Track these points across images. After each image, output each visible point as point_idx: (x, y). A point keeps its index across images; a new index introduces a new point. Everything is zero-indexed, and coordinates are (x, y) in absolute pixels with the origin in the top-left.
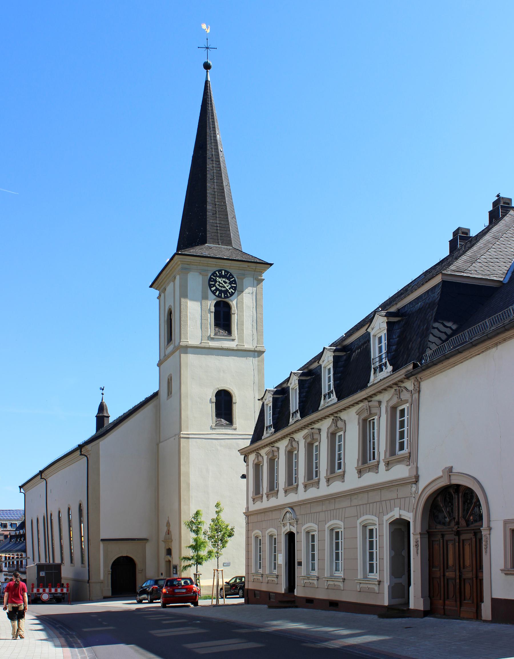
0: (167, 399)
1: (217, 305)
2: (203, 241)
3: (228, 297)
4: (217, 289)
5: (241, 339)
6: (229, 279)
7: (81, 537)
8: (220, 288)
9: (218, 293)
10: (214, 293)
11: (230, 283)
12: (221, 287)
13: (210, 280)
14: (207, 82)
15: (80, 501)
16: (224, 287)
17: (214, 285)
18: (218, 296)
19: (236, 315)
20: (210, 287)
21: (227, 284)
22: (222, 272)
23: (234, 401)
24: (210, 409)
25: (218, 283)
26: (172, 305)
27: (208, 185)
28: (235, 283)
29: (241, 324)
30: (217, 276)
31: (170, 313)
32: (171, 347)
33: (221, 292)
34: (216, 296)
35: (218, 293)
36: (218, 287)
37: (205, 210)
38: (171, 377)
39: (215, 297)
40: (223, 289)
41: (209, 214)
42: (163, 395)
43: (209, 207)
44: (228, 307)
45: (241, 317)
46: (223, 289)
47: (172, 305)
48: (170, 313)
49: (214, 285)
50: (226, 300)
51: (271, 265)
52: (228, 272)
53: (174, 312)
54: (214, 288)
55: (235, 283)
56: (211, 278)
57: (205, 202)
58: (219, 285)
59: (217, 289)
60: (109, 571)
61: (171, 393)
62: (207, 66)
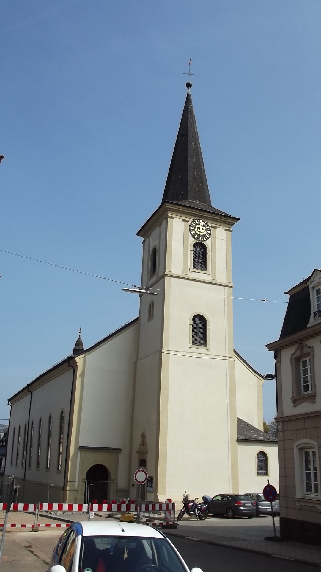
0: (148, 321)
1: (196, 245)
2: (185, 198)
4: (196, 233)
5: (214, 274)
7: (60, 443)
8: (198, 233)
9: (196, 236)
10: (193, 236)
11: (206, 230)
15: (63, 409)
17: (194, 230)
19: (210, 255)
20: (190, 232)
23: (208, 325)
24: (188, 330)
25: (196, 229)
26: (157, 245)
27: (189, 159)
28: (210, 231)
29: (214, 262)
31: (155, 251)
32: (155, 279)
35: (196, 236)
37: (187, 176)
38: (153, 303)
39: (194, 239)
41: (190, 179)
42: (144, 320)
43: (190, 175)
44: (204, 247)
45: (214, 257)
47: (157, 245)
48: (155, 251)
49: (194, 230)
51: (238, 219)
53: (159, 251)
54: (193, 232)
55: (210, 231)
56: (191, 224)
57: (187, 170)
60: (83, 479)
61: (153, 316)
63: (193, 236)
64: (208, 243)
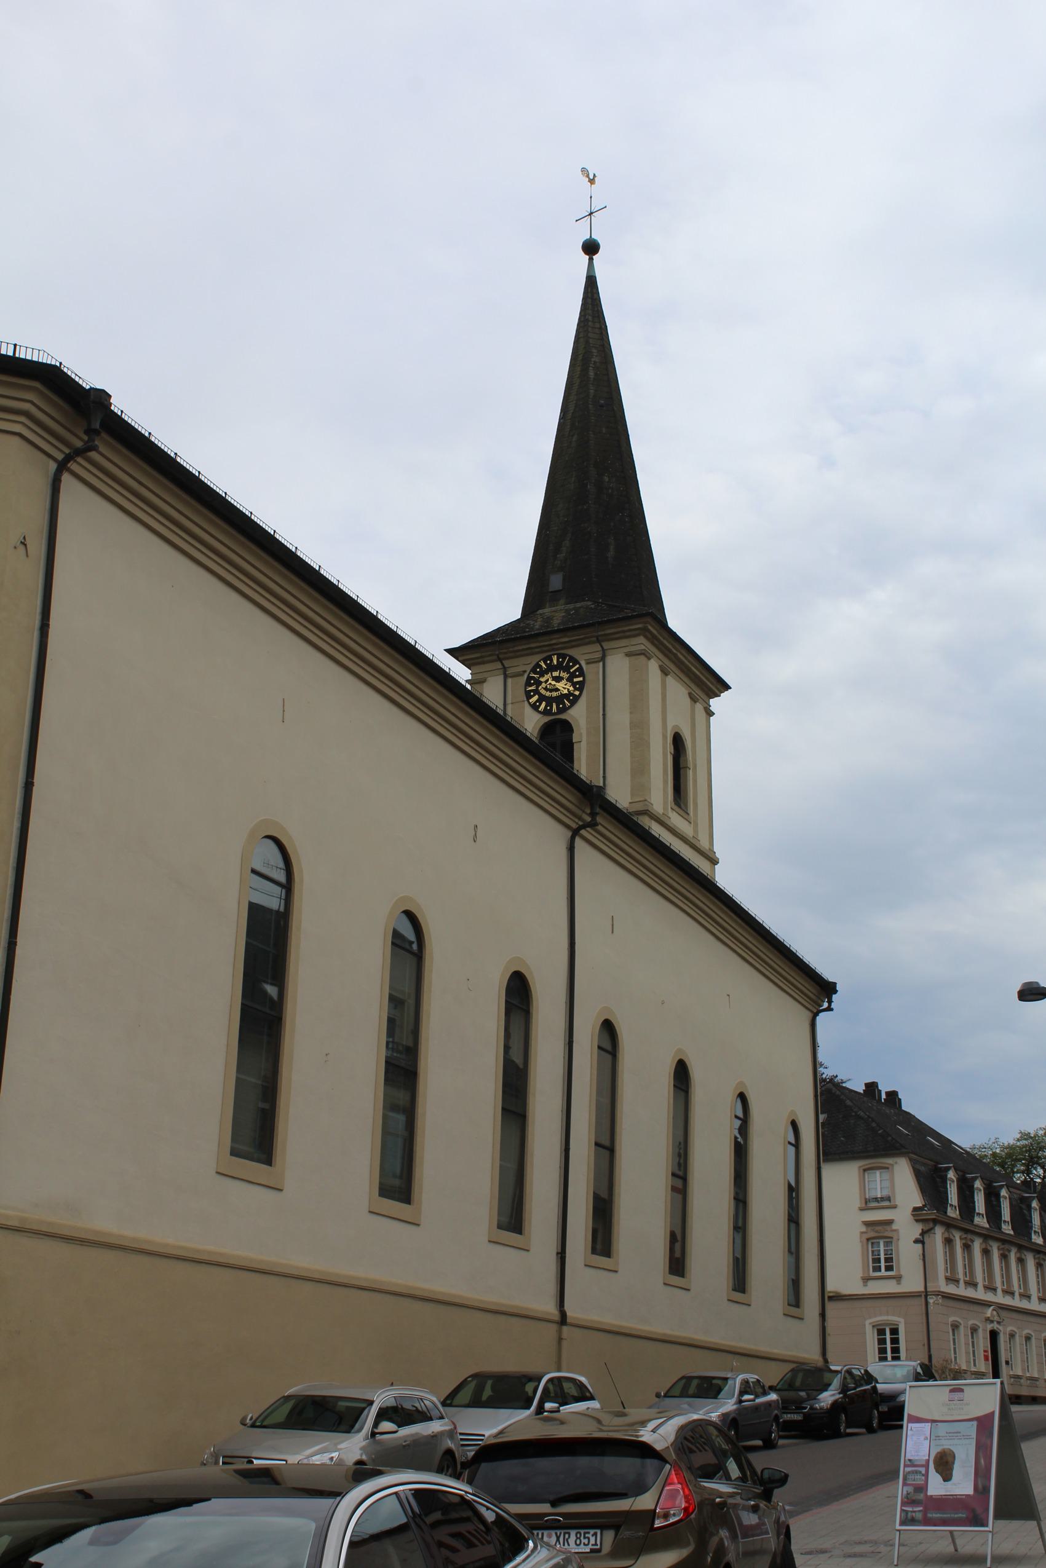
3: (565, 709)
4: (542, 698)
6: (567, 669)
8: (548, 694)
11: (570, 680)
12: (551, 691)
13: (528, 684)
14: (591, 284)
16: (557, 690)
18: (546, 712)
19: (584, 745)
21: (564, 681)
22: (552, 660)
25: (544, 685)
30: (543, 673)
33: (549, 701)
34: (540, 712)
36: (543, 692)
39: (540, 716)
40: (555, 694)
44: (567, 727)
46: (555, 694)
50: (563, 716)
52: (564, 656)
58: (546, 689)
59: (540, 701)
62: (591, 248)
63: (535, 707)
64: (578, 715)
